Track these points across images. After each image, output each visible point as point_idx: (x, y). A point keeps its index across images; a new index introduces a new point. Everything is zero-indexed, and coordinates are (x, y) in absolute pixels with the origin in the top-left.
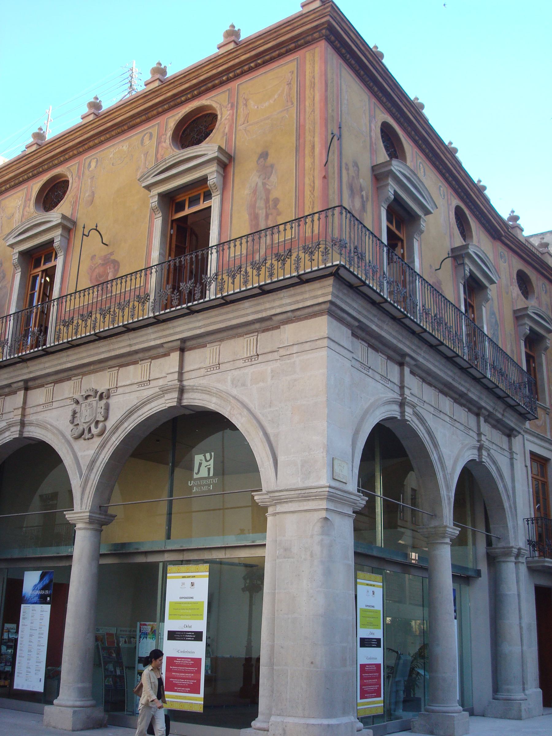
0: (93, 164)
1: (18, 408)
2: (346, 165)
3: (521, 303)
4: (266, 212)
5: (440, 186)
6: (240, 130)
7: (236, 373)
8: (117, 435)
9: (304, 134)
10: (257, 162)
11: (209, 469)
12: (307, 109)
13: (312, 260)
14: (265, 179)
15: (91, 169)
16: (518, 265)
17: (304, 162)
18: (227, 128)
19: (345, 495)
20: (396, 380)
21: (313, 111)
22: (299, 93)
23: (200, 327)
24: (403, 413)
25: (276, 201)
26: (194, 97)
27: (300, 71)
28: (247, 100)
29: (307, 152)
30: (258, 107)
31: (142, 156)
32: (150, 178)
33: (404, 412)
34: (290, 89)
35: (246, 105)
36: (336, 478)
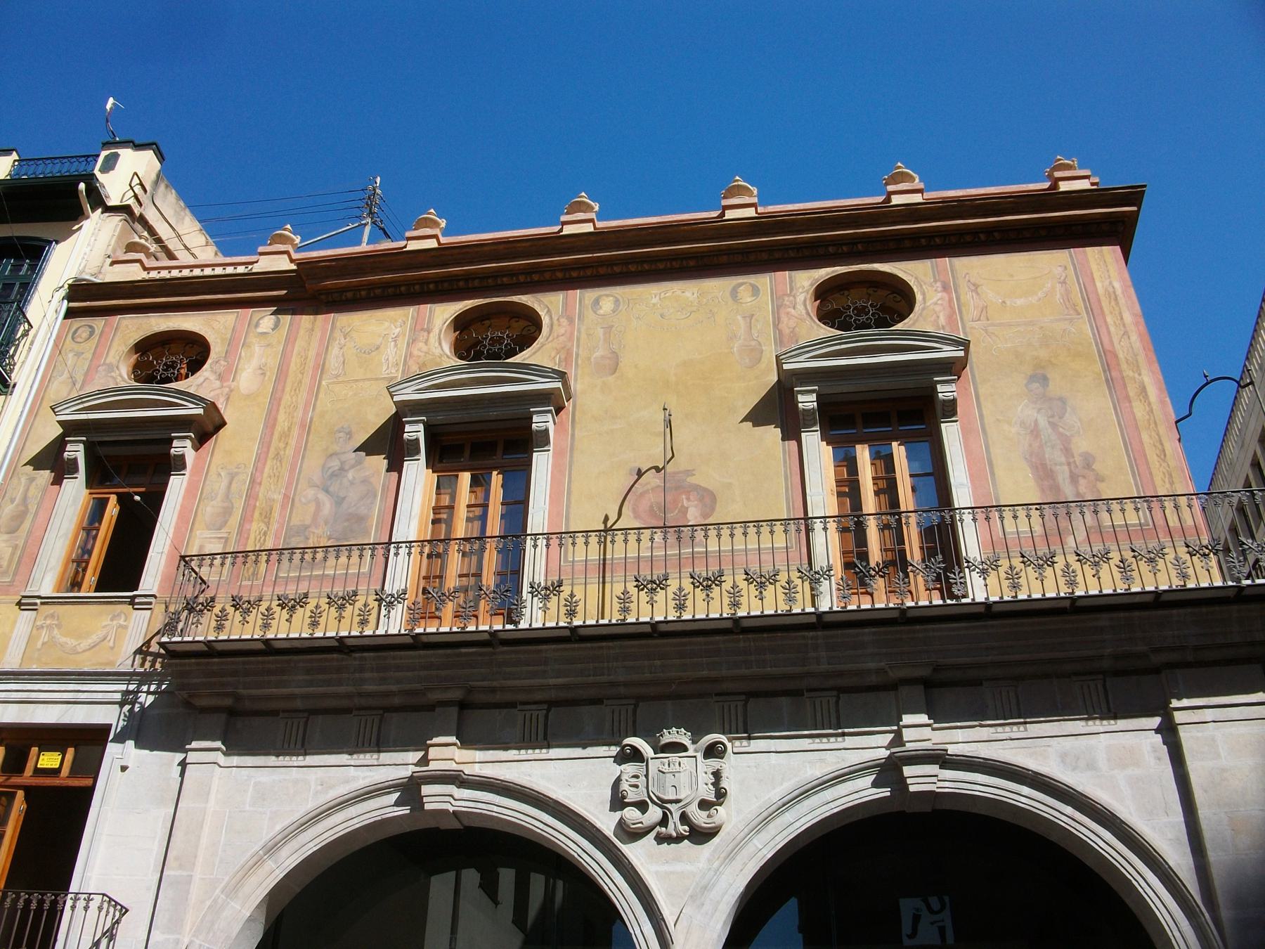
0: (607, 305)
4: (1071, 472)
8: (765, 836)
9: (1119, 365)
10: (1026, 385)
11: (942, 930)
12: (1112, 329)
14: (1053, 416)
15: (601, 312)
17: (1131, 407)
21: (1126, 333)
22: (1087, 299)
25: (1088, 461)
31: (739, 317)
35: (976, 291)
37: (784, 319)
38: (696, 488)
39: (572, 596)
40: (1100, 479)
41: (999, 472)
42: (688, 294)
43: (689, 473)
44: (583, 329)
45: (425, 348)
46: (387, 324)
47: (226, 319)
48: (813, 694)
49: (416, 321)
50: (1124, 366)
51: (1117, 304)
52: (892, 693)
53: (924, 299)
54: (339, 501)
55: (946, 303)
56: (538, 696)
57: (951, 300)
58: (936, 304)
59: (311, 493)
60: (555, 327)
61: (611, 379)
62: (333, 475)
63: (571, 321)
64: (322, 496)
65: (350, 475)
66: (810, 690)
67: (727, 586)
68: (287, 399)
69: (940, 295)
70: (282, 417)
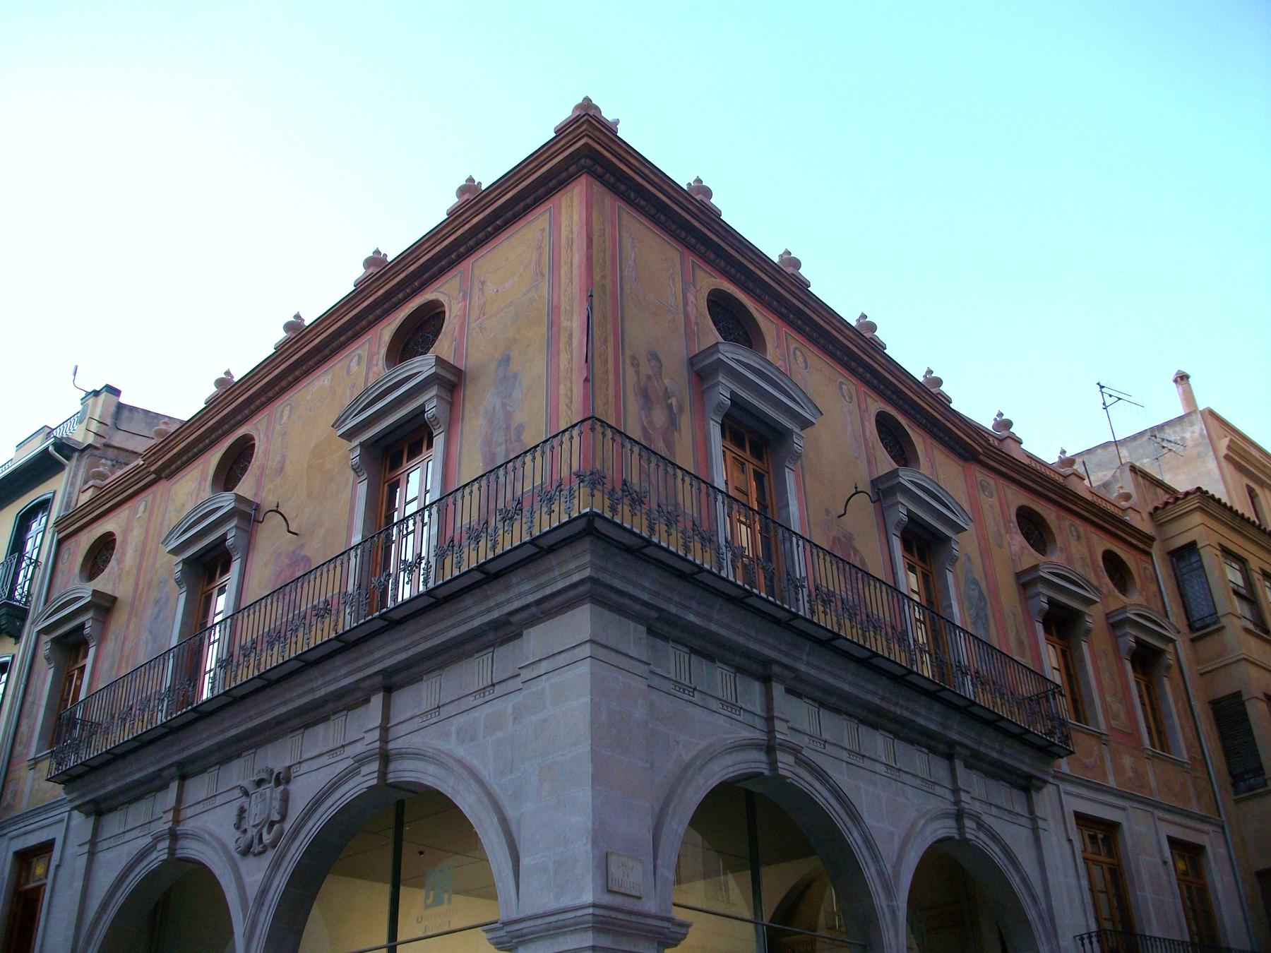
0: (286, 413)
2: (634, 358)
3: (1030, 557)
5: (842, 383)
7: (462, 719)
12: (563, 280)
13: (551, 512)
16: (1018, 498)
19: (633, 918)
20: (758, 708)
23: (406, 649)
24: (773, 764)
27: (555, 226)
28: (483, 283)
33: (776, 761)
34: (540, 255)
35: (482, 290)
36: (615, 888)
47: (123, 514)
68: (144, 565)
70: (141, 582)
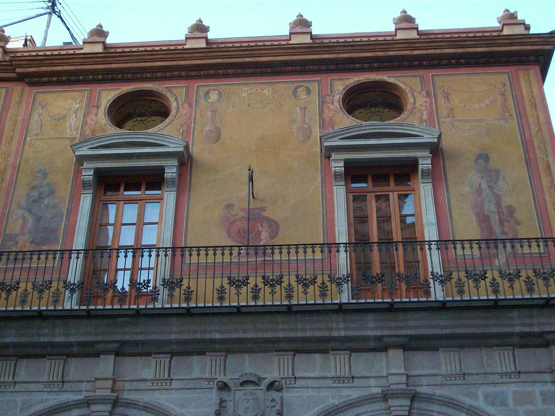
0: (214, 97)
1: (106, 379)
4: (500, 218)
6: (444, 122)
7: (491, 389)
12: (532, 127)
14: (491, 182)
15: (210, 101)
18: (425, 114)
21: (540, 130)
23: (442, 327)
25: (511, 210)
26: (372, 69)
29: (541, 169)
30: (465, 106)
31: (298, 109)
32: (336, 139)
34: (505, 100)
37: (326, 111)
38: (268, 219)
39: (189, 287)
40: (518, 223)
41: (455, 216)
42: (266, 91)
43: (263, 209)
44: (198, 111)
45: (95, 119)
46: (70, 101)
48: (335, 352)
49: (90, 99)
50: (537, 151)
51: (536, 111)
52: (384, 353)
53: (415, 102)
54: (39, 219)
55: (428, 105)
56: (166, 349)
57: (431, 103)
58: (421, 105)
59: (20, 212)
60: (180, 109)
61: (216, 145)
62: (35, 201)
63: (190, 105)
64: (27, 215)
65: (46, 202)
66: (332, 350)
67: (285, 284)
69: (424, 99)
